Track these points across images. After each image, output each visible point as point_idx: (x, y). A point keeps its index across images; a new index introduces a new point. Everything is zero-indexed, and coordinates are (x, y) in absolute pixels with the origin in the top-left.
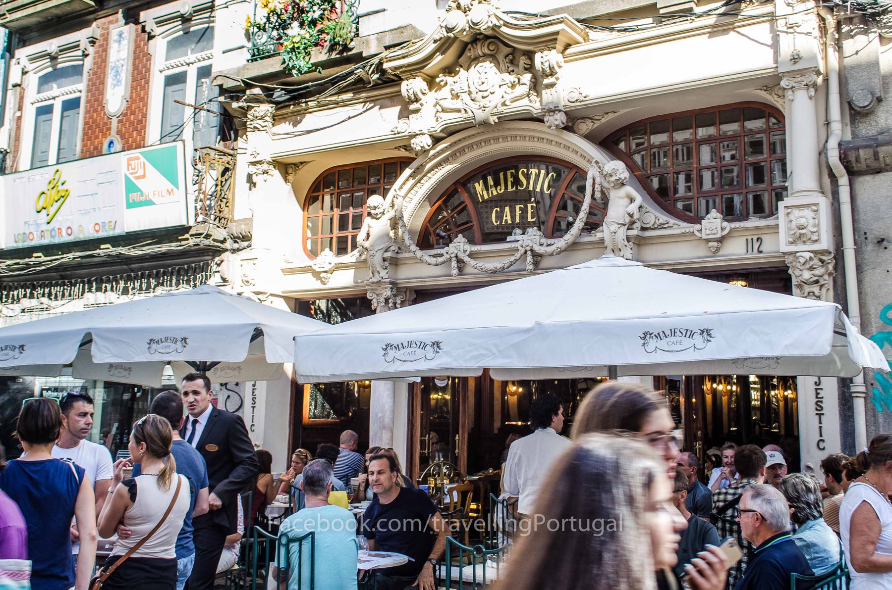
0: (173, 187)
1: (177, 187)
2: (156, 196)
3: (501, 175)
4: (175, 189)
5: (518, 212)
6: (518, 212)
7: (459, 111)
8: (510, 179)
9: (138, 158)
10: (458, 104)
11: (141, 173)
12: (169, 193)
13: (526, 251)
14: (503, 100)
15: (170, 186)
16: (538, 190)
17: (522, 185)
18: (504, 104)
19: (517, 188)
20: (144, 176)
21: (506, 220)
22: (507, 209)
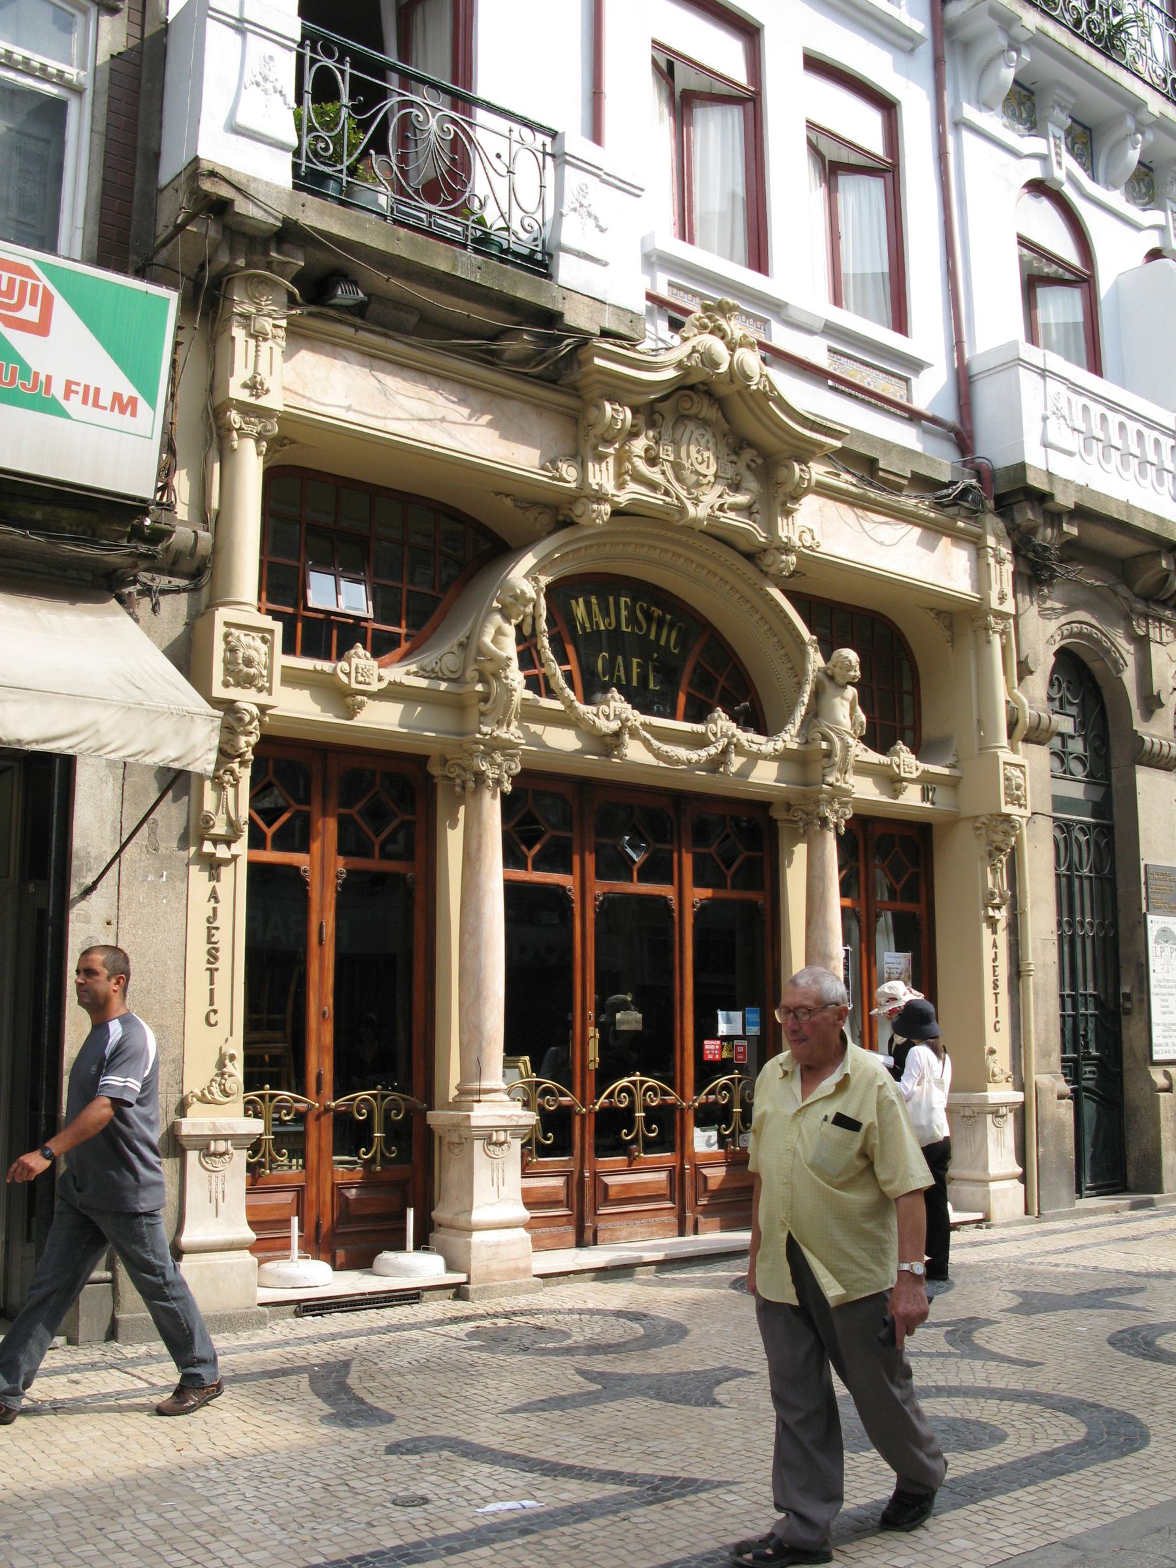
0: (135, 393)
1: (153, 406)
2: (76, 399)
3: (611, 599)
4: (142, 404)
5: (635, 670)
6: (635, 670)
7: (653, 486)
8: (624, 613)
9: (26, 271)
10: (654, 474)
11: (31, 313)
12: (123, 405)
13: (729, 743)
14: (722, 501)
15: (128, 390)
16: (662, 642)
17: (640, 629)
18: (721, 508)
19: (633, 629)
20: (42, 328)
21: (619, 677)
22: (620, 659)
